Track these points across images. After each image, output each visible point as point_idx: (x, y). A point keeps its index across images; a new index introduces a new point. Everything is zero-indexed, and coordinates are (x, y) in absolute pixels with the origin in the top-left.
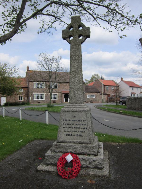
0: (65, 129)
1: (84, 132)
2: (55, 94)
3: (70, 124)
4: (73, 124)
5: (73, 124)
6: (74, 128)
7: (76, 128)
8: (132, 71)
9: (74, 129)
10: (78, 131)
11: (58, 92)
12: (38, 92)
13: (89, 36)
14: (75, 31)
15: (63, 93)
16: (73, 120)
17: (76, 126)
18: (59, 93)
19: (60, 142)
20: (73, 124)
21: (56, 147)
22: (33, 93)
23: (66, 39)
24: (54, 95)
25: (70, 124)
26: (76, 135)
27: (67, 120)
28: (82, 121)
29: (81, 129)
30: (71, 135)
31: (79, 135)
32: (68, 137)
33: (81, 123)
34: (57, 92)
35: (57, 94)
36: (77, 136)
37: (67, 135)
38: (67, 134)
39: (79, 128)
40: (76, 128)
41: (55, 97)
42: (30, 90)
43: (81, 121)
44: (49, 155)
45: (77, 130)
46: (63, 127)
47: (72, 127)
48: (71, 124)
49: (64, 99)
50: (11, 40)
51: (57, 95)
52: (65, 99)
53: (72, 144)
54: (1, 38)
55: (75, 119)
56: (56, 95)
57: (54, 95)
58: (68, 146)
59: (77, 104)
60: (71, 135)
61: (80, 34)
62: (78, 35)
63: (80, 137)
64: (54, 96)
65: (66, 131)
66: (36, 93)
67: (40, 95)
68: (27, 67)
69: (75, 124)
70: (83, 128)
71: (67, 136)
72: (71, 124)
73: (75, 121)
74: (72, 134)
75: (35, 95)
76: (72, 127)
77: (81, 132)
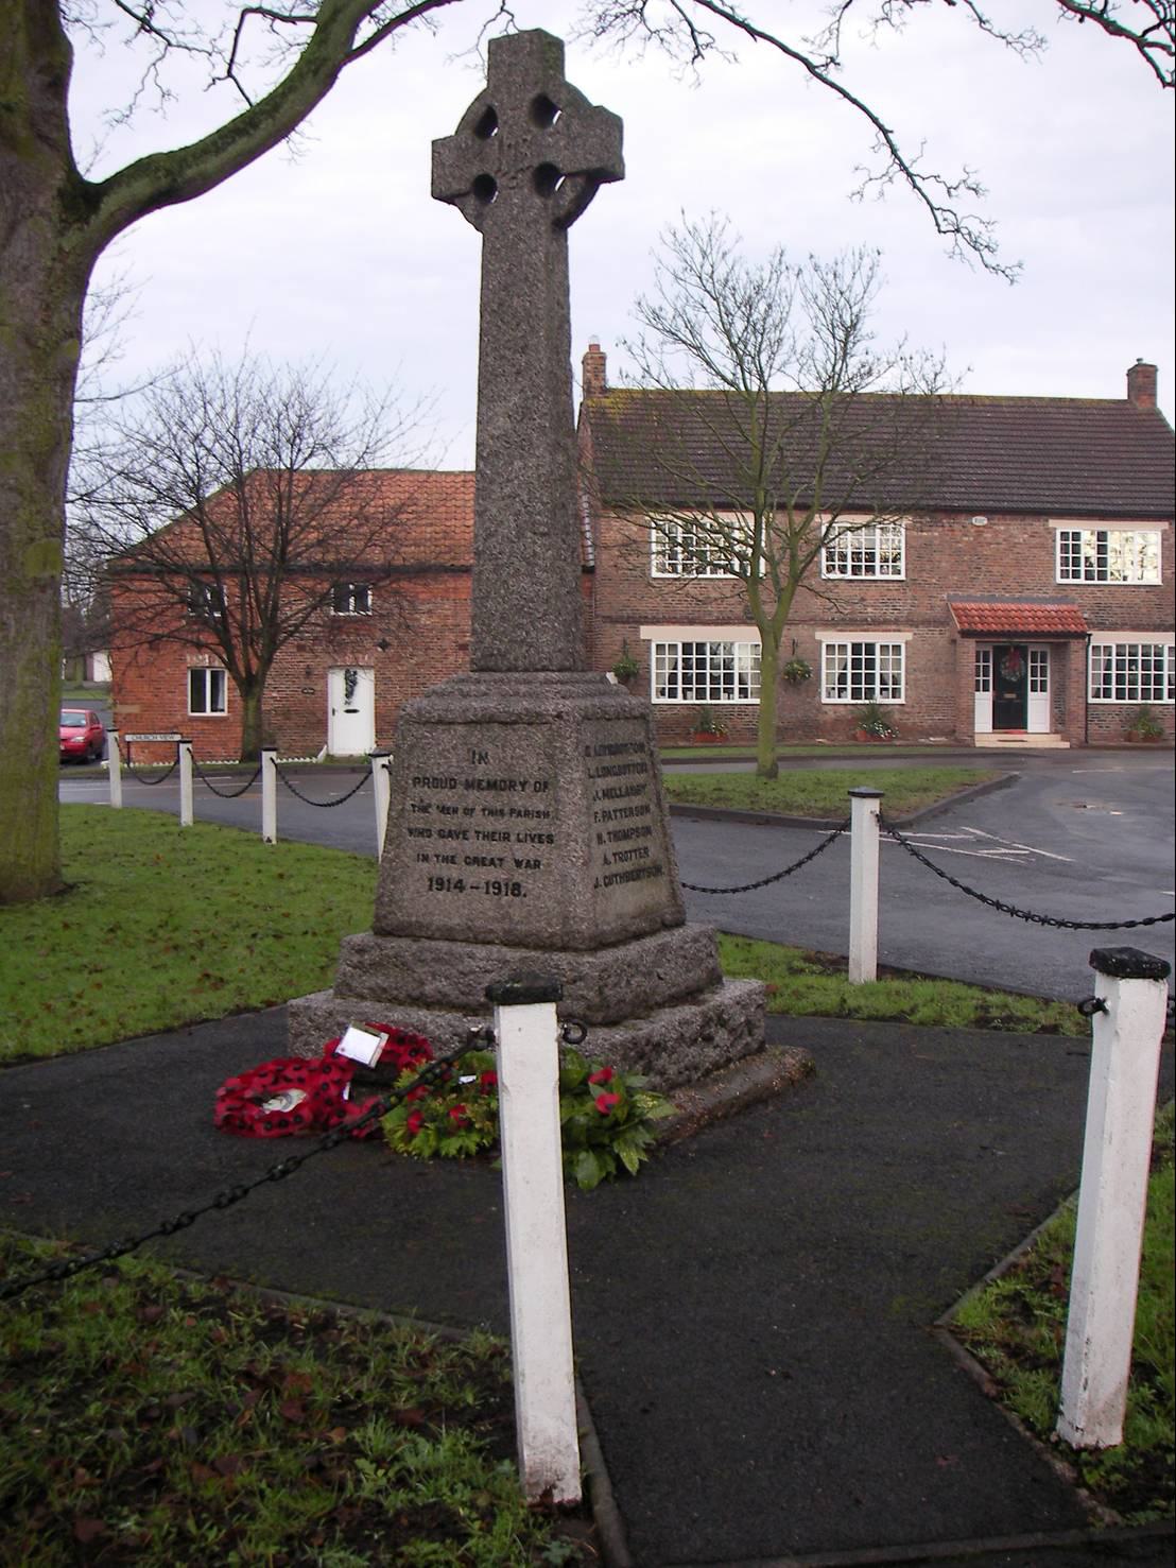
0: (422, 841)
1: (537, 864)
2: (878, 638)
3: (455, 811)
4: (469, 812)
5: (473, 810)
6: (477, 832)
7: (490, 836)
8: (344, 436)
9: (474, 847)
10: (501, 860)
11: (911, 623)
12: (692, 622)
13: (614, 174)
14: (509, 146)
15: (965, 634)
16: (470, 779)
17: (491, 824)
18: (922, 630)
19: (389, 929)
20: (469, 812)
21: (356, 959)
22: (646, 632)
23: (456, 201)
24: (870, 648)
25: (455, 811)
26: (487, 883)
27: (436, 783)
28: (523, 785)
29: (519, 841)
30: (455, 887)
31: (503, 889)
32: (440, 895)
33: (519, 799)
34: (896, 622)
35: (901, 638)
36: (491, 890)
37: (435, 886)
38: (431, 880)
39: (506, 837)
40: (490, 836)
41: (877, 672)
42: (611, 598)
43: (519, 788)
44: (309, 1007)
45: (496, 849)
46: (411, 832)
47: (465, 833)
48: (460, 811)
49: (984, 703)
50: (1081, 20)
51: (897, 648)
52: (1047, 695)
53: (459, 948)
54: (71, 240)
55: (481, 772)
56: (884, 648)
57: (870, 648)
58: (428, 956)
59: (516, 669)
60: (460, 886)
61: (542, 160)
62: (529, 174)
63: (511, 897)
64: (870, 664)
65: (426, 858)
66: (678, 635)
67: (687, 648)
68: (1131, 373)
69: (484, 810)
70: (533, 840)
71: (430, 889)
72: (460, 811)
73: (484, 784)
74: (460, 881)
75: (660, 647)
76: (465, 833)
77: (518, 863)
